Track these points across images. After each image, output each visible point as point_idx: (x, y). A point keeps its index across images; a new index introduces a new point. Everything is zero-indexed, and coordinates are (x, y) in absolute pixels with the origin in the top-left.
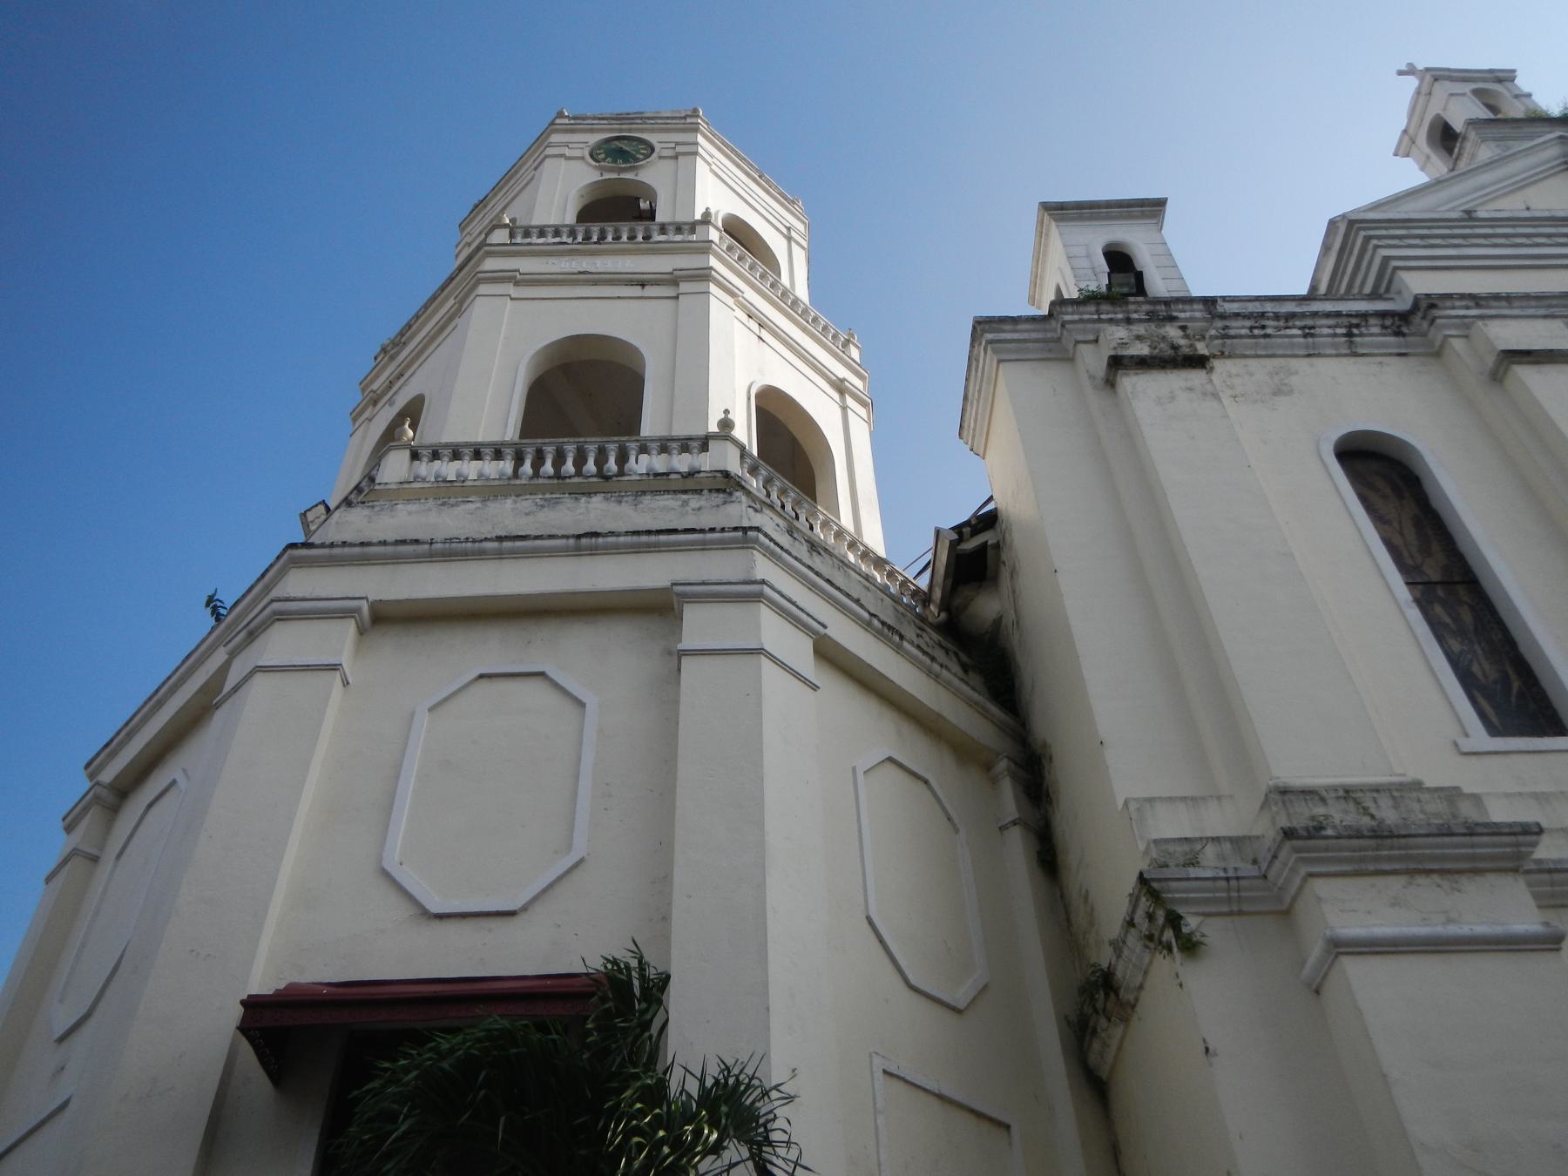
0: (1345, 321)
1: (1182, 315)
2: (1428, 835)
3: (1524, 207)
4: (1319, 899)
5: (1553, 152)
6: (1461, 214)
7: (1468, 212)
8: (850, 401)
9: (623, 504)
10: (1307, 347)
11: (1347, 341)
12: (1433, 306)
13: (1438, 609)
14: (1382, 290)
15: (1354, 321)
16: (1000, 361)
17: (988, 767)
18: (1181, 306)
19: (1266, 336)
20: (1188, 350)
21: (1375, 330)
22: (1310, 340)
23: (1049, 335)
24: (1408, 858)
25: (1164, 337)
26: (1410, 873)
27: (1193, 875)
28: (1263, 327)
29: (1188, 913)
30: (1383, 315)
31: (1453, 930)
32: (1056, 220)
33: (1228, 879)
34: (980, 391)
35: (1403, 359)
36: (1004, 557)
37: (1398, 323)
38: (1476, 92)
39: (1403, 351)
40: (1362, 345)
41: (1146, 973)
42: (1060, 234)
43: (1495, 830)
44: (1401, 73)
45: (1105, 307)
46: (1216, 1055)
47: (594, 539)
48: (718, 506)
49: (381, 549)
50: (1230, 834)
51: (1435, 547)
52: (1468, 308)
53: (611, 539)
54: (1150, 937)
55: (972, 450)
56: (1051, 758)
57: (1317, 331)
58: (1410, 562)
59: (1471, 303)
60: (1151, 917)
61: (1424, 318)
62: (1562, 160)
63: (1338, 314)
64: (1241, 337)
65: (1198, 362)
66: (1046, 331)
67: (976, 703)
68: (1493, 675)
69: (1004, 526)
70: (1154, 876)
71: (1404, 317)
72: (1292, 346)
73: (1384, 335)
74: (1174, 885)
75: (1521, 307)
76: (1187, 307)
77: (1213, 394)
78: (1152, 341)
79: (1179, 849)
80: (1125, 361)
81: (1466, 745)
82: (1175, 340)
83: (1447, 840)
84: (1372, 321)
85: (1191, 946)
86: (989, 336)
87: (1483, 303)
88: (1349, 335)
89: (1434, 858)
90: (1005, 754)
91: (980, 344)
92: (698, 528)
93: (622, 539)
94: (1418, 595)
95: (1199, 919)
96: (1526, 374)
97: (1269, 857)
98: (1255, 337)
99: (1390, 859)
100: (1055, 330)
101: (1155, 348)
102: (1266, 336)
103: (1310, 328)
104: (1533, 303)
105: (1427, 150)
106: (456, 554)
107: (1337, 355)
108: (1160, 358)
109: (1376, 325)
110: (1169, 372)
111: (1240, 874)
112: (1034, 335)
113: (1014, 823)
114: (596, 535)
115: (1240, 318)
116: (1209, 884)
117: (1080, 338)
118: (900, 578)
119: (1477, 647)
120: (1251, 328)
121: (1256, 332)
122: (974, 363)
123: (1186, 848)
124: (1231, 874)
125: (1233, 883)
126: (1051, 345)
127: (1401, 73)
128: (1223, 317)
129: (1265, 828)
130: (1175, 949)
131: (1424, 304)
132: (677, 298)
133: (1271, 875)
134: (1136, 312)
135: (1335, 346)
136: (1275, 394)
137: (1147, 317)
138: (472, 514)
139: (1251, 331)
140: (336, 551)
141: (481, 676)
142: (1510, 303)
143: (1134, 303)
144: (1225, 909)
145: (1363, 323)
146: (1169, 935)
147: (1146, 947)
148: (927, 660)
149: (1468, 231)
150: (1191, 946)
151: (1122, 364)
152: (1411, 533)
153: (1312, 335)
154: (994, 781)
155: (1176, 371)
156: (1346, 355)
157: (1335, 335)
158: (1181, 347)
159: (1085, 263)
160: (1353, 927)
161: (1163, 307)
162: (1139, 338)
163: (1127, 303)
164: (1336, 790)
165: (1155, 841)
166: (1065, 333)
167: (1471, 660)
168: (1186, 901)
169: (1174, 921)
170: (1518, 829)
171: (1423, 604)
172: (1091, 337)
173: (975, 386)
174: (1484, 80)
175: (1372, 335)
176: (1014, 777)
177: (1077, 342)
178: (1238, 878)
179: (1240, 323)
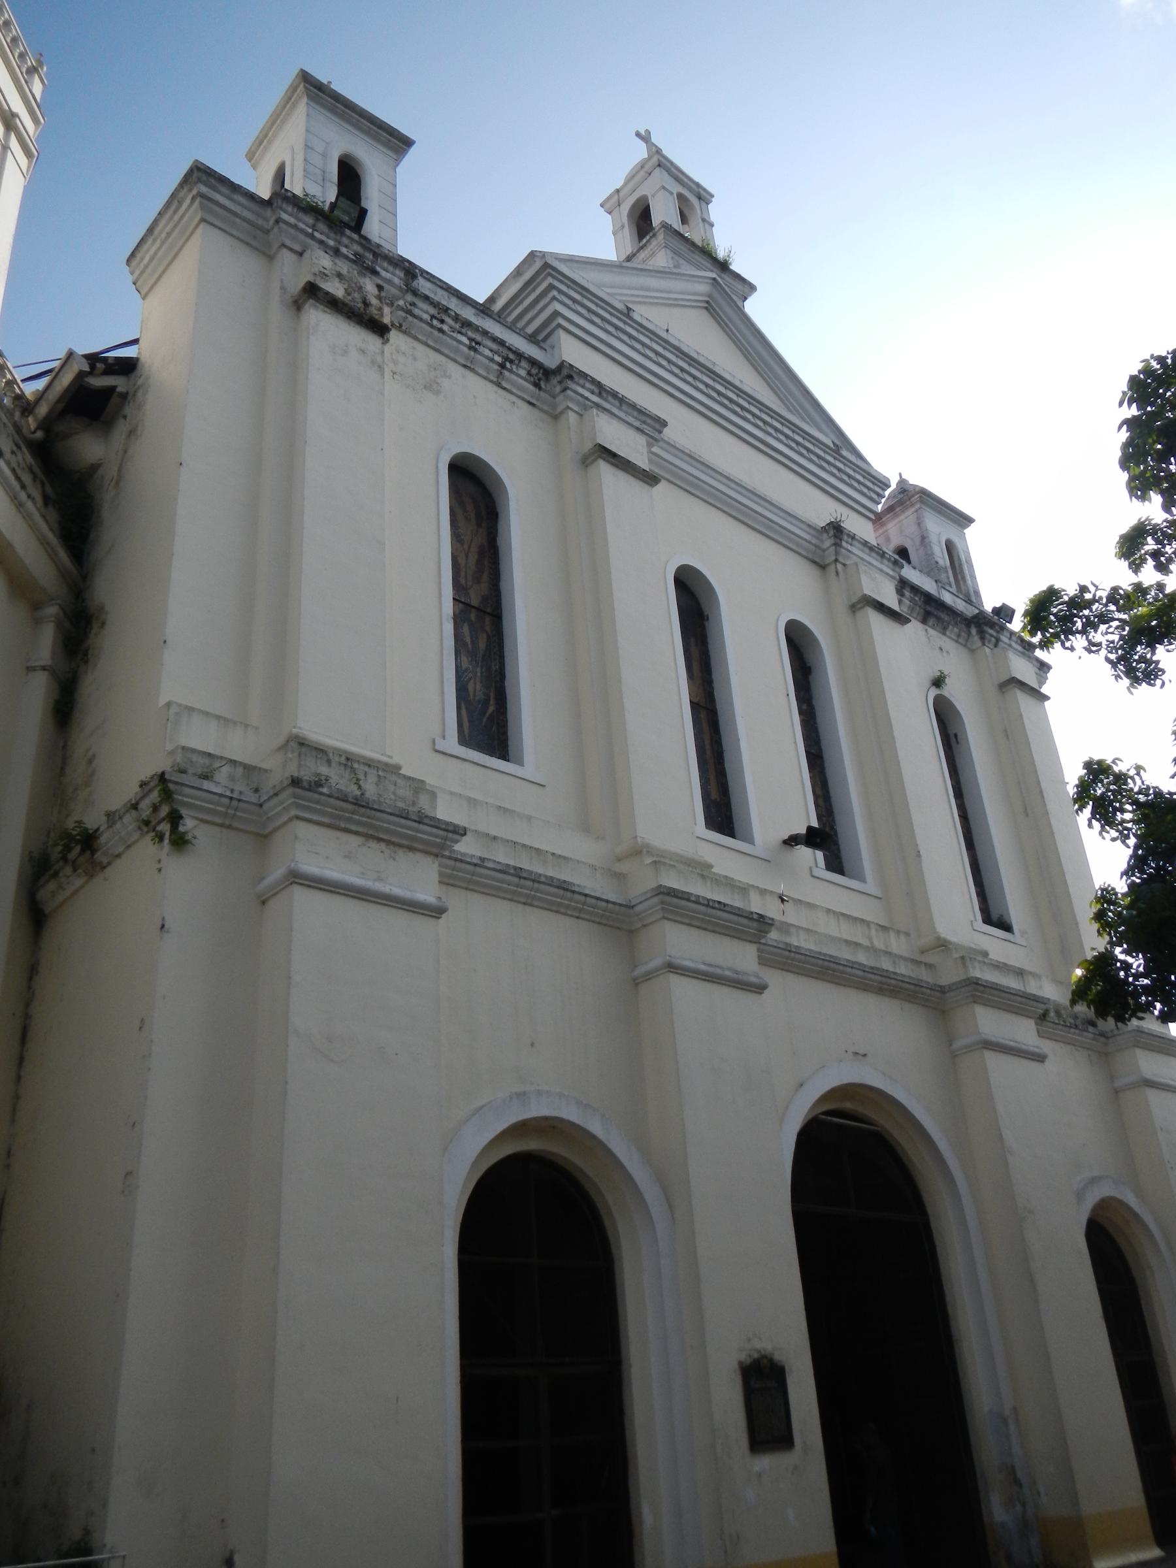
0: (505, 352)
1: (383, 273)
2: (391, 814)
3: (666, 328)
4: (296, 838)
5: (704, 288)
6: (624, 308)
7: (629, 309)
8: (14, 143)
10: (467, 359)
11: (498, 370)
12: (570, 377)
13: (466, 629)
14: (540, 337)
15: (511, 356)
16: (203, 220)
17: (36, 606)
18: (385, 264)
19: (441, 331)
20: (376, 312)
21: (523, 373)
22: (472, 353)
23: (260, 222)
24: (371, 826)
25: (360, 288)
26: (368, 837)
27: (205, 787)
28: (442, 321)
29: (189, 815)
30: (533, 362)
31: (378, 887)
32: (309, 97)
33: (231, 798)
34: (169, 234)
35: (530, 408)
36: (127, 410)
38: (680, 197)
40: (508, 380)
41: (129, 847)
42: (308, 115)
43: (437, 824)
44: (638, 134)
45: (322, 226)
46: (168, 932)
50: (247, 761)
51: (485, 578)
52: (593, 393)
54: (147, 823)
55: (134, 284)
56: (103, 624)
57: (481, 349)
58: (463, 581)
59: (597, 391)
60: (155, 808)
61: (560, 382)
62: (707, 299)
63: (502, 343)
64: (421, 320)
65: (379, 329)
66: (258, 215)
67: (48, 544)
68: (480, 695)
69: (140, 382)
70: (173, 779)
71: (547, 373)
72: (457, 351)
73: (526, 380)
74: (187, 790)
75: (626, 413)
76: (391, 268)
77: (379, 367)
78: (349, 286)
79: (202, 761)
80: (320, 294)
81: (441, 745)
82: (369, 296)
83: (403, 821)
84: (524, 364)
85: (180, 842)
86: (204, 189)
87: (604, 394)
88: (502, 366)
89: (387, 831)
90: (58, 601)
91: (190, 190)
94: (457, 612)
95: (195, 822)
96: (604, 469)
97: (271, 793)
98: (432, 326)
99: (358, 823)
100: (267, 220)
101: (349, 294)
102: (441, 331)
103: (477, 343)
104: (635, 413)
105: (625, 219)
107: (485, 378)
108: (351, 308)
109: (525, 369)
110: (352, 324)
111: (243, 798)
112: (246, 214)
113: (44, 668)
115: (428, 302)
116: (216, 797)
117: (288, 243)
118: (9, 376)
119: (479, 670)
120: (433, 317)
121: (435, 322)
122: (175, 204)
123: (207, 761)
124: (235, 795)
125: (234, 803)
126: (258, 232)
127: (638, 134)
128: (415, 293)
129: (278, 769)
130: (166, 841)
131: (565, 372)
133: (266, 807)
134: (346, 247)
135: (487, 369)
136: (425, 387)
137: (354, 258)
139: (431, 320)
142: (621, 405)
143: (349, 238)
144: (219, 821)
145: (517, 362)
146: (165, 827)
147: (140, 828)
148: (17, 486)
149: (621, 325)
150: (180, 842)
151: (315, 295)
152: (473, 557)
153: (475, 350)
154: (37, 622)
155: (358, 327)
156: (491, 381)
157: (492, 360)
158: (372, 305)
159: (317, 160)
160: (311, 867)
161: (371, 257)
162: (339, 275)
163: (342, 234)
164: (341, 755)
165: (183, 748)
166: (276, 230)
167: (470, 679)
168: (190, 806)
169: (175, 818)
170: (451, 828)
171: (458, 620)
172: (298, 248)
173: (166, 225)
174: (690, 190)
175: (518, 375)
176: (59, 625)
177: (283, 245)
178: (239, 800)
179: (424, 306)
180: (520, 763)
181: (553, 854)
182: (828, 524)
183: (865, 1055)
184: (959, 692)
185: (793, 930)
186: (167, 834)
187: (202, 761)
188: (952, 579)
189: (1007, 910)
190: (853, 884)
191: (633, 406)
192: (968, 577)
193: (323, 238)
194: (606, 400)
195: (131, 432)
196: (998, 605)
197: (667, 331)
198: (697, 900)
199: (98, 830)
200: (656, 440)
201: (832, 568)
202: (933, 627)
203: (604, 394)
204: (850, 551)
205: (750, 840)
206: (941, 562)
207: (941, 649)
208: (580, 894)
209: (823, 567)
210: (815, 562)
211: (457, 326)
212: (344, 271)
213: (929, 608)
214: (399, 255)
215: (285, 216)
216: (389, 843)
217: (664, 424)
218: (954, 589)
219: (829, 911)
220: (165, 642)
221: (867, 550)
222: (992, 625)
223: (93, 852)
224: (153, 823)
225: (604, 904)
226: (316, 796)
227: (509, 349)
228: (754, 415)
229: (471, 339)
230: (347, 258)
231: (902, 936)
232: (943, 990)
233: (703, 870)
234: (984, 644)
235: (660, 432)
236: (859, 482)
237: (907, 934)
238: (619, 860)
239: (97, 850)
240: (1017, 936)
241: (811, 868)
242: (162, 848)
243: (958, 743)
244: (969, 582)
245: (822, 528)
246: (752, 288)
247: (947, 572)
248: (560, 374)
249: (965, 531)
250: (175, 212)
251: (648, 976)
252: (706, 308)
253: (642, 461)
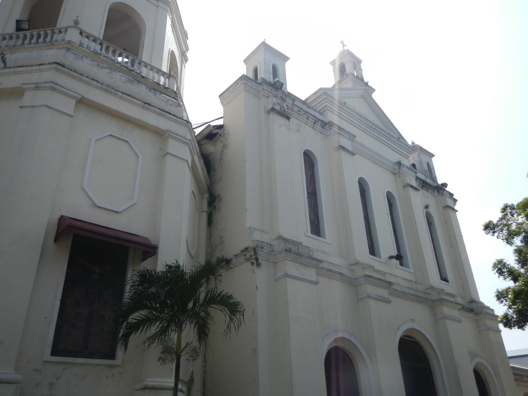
1: (287, 101)
3: (354, 107)
7: (345, 103)
9: (151, 92)
15: (317, 120)
16: (244, 90)
19: (300, 114)
21: (319, 124)
25: (283, 107)
27: (264, 251)
30: (322, 121)
31: (304, 277)
33: (269, 254)
37: (324, 125)
38: (354, 62)
39: (322, 132)
41: (241, 264)
43: (315, 259)
45: (273, 89)
47: (149, 106)
48: (176, 106)
49: (86, 79)
52: (337, 129)
53: (153, 108)
54: (248, 259)
57: (309, 119)
62: (362, 95)
63: (314, 117)
65: (288, 118)
69: (225, 132)
73: (320, 126)
77: (289, 129)
80: (275, 110)
84: (320, 122)
86: (245, 82)
88: (314, 123)
91: (241, 81)
92: (177, 116)
93: (156, 109)
96: (342, 151)
97: (279, 253)
98: (297, 113)
102: (300, 114)
103: (309, 117)
106: (109, 92)
113: (206, 211)
114: (149, 104)
115: (297, 107)
119: (312, 211)
120: (298, 111)
121: (298, 112)
122: (236, 85)
124: (270, 253)
125: (270, 255)
131: (331, 124)
132: (158, 6)
133: (277, 256)
134: (279, 94)
136: (297, 131)
137: (280, 97)
138: (107, 74)
140: (72, 73)
141: (110, 135)
142: (344, 132)
143: (279, 92)
144: (266, 259)
145: (318, 121)
146: (255, 261)
147: (245, 260)
150: (258, 265)
153: (308, 119)
157: (312, 121)
160: (290, 273)
162: (278, 104)
164: (291, 241)
175: (318, 125)
177: (264, 95)
180: (325, 238)
181: (337, 265)
182: (397, 162)
183: (414, 320)
184: (432, 210)
185: (394, 284)
186: (255, 263)
187: (260, 243)
188: (429, 174)
189: (447, 275)
190: (407, 269)
191: (348, 132)
192: (433, 173)
193: (273, 93)
194: (341, 131)
195: (224, 146)
196: (443, 183)
197: (355, 108)
198: (375, 278)
199: (232, 259)
200: (353, 141)
201: (398, 175)
202: (425, 190)
203: (340, 129)
204: (403, 170)
205: (380, 257)
206: (426, 169)
207: (427, 197)
208: (345, 276)
209: (395, 174)
210: (393, 173)
211: (304, 113)
212: (279, 102)
213: (424, 185)
214: (288, 91)
215: (265, 88)
216: (305, 265)
217: (355, 136)
218: (429, 178)
219: (402, 278)
220: (246, 210)
221: (407, 169)
222: (441, 189)
223: (229, 265)
224: (250, 259)
225: (350, 279)
226: (290, 254)
227: (316, 118)
228: (377, 130)
229: (307, 116)
230: (279, 97)
231: (421, 285)
232: (433, 301)
233: (372, 267)
234: (439, 195)
235: (354, 139)
236: (404, 148)
237: (422, 284)
238: (351, 265)
239: (230, 264)
240: (450, 284)
241: (396, 265)
242: (254, 267)
243: (431, 224)
244: (434, 175)
245: (395, 163)
246: (374, 90)
247: (427, 172)
248: (329, 124)
249: (432, 159)
250: (236, 86)
251: (362, 299)
252: (362, 97)
253: (350, 148)
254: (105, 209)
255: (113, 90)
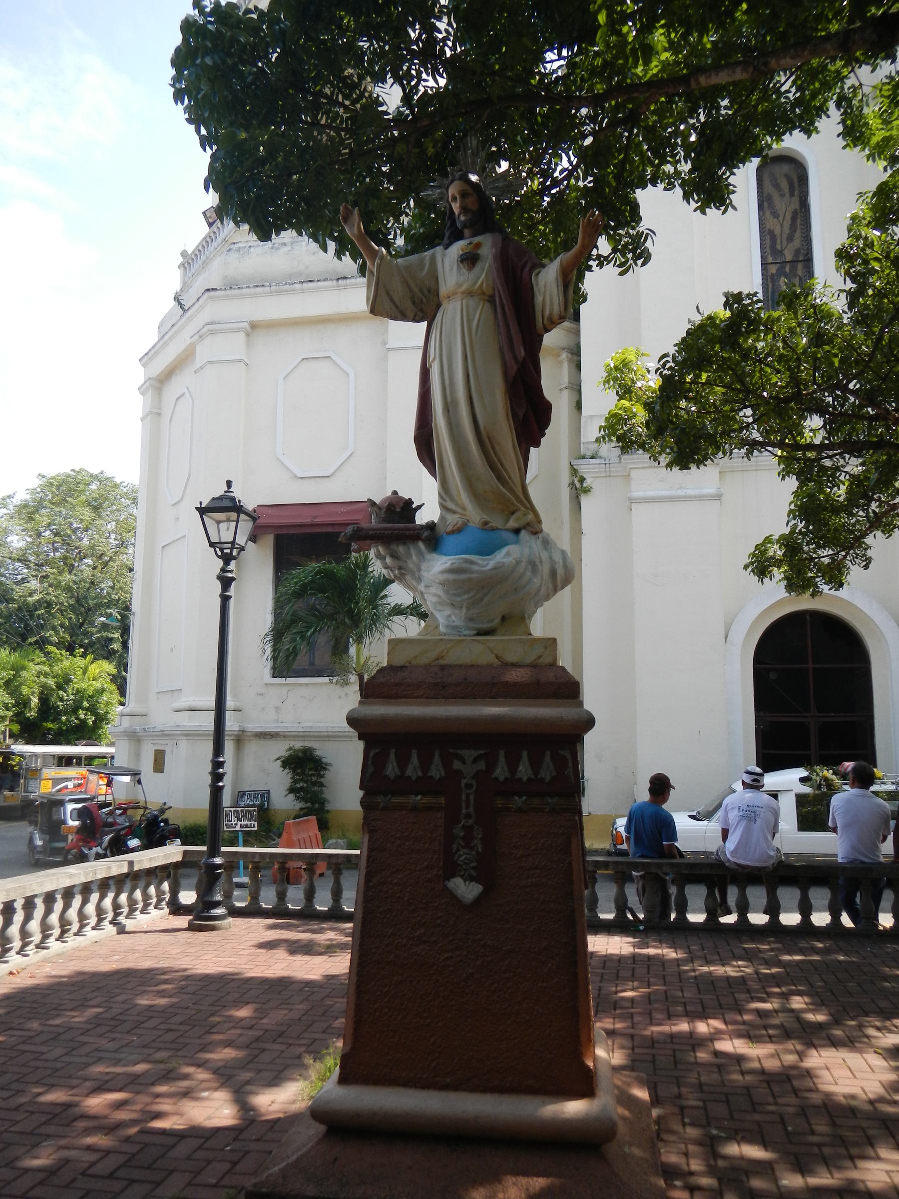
254: (311, 477)
255: (288, 286)
